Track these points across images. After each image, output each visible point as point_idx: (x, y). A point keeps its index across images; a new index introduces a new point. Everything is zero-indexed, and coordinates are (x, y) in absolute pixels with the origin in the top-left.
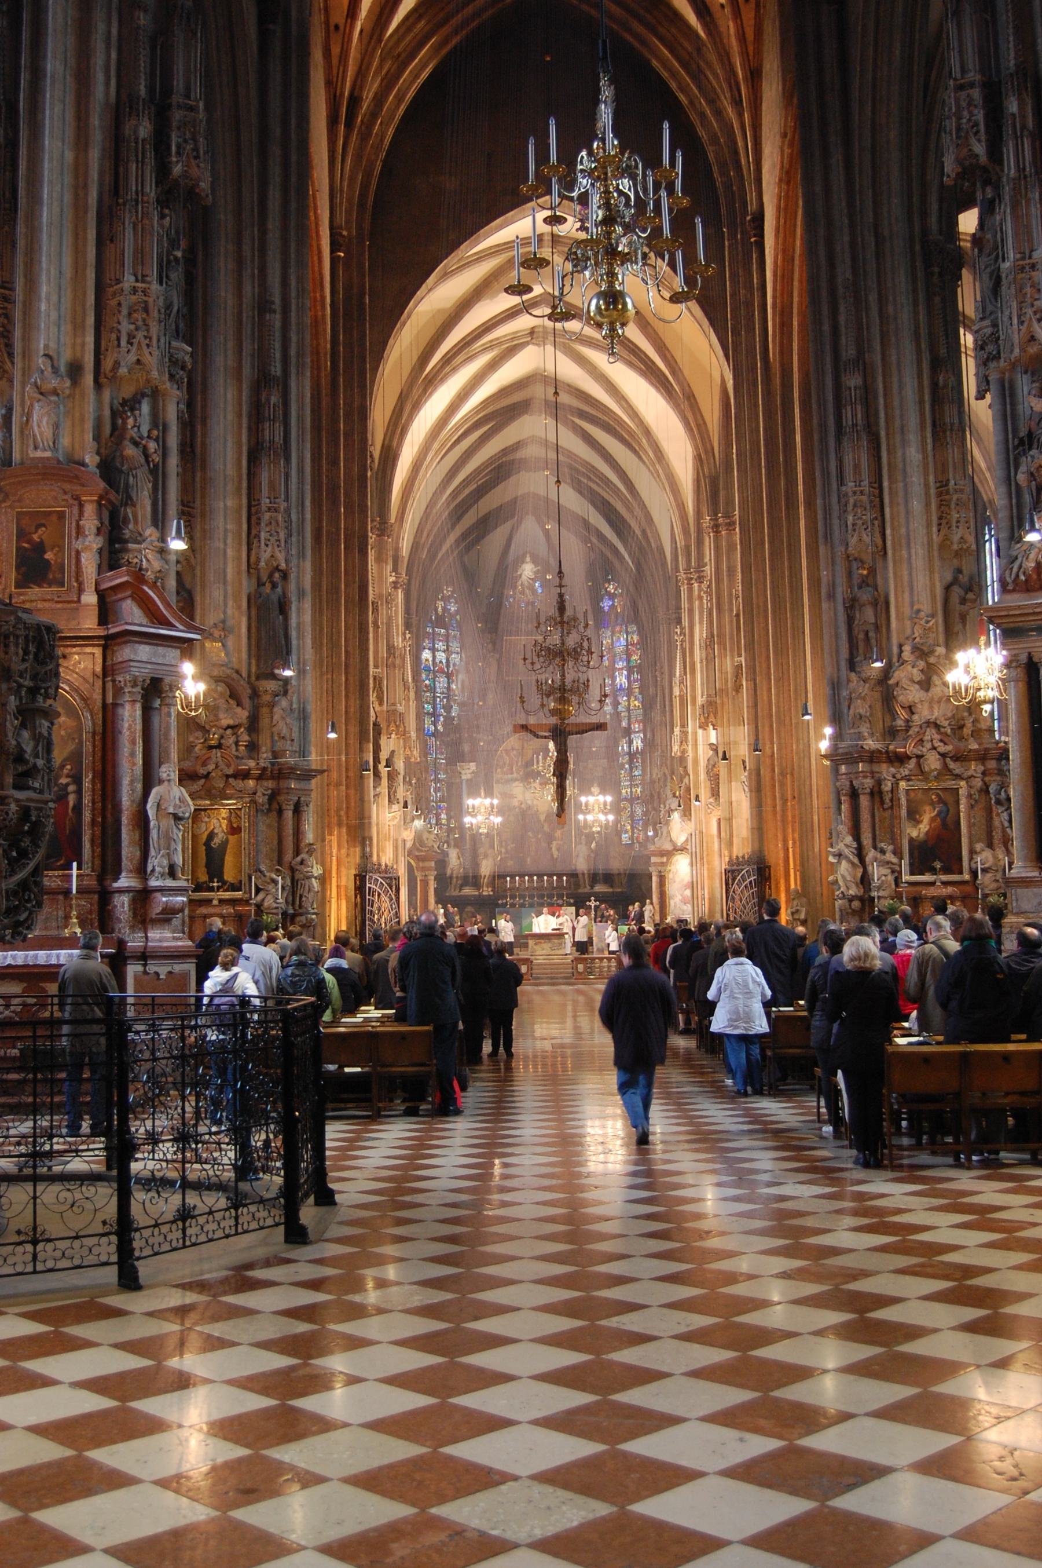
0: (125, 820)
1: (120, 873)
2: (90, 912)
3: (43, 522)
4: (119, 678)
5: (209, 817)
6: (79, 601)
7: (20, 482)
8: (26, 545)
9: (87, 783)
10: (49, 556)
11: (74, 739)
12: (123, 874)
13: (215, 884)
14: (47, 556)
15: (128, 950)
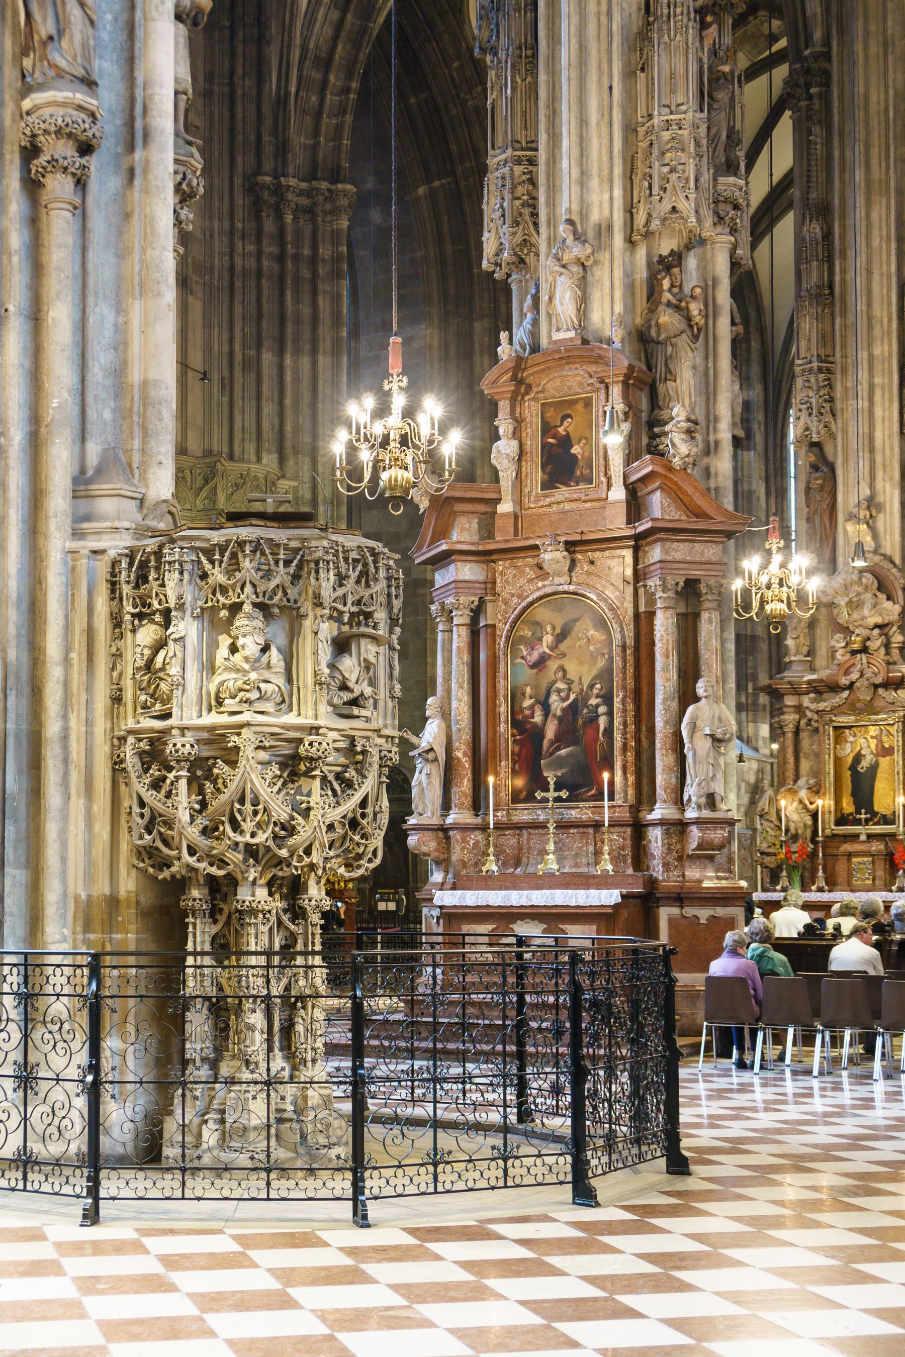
0: (658, 745)
1: (655, 803)
2: (623, 848)
3: (569, 412)
4: (650, 583)
5: (855, 736)
6: (607, 499)
7: (543, 371)
8: (551, 440)
9: (617, 702)
10: (576, 450)
11: (603, 654)
12: (658, 805)
13: (863, 816)
14: (573, 451)
15: (661, 890)
